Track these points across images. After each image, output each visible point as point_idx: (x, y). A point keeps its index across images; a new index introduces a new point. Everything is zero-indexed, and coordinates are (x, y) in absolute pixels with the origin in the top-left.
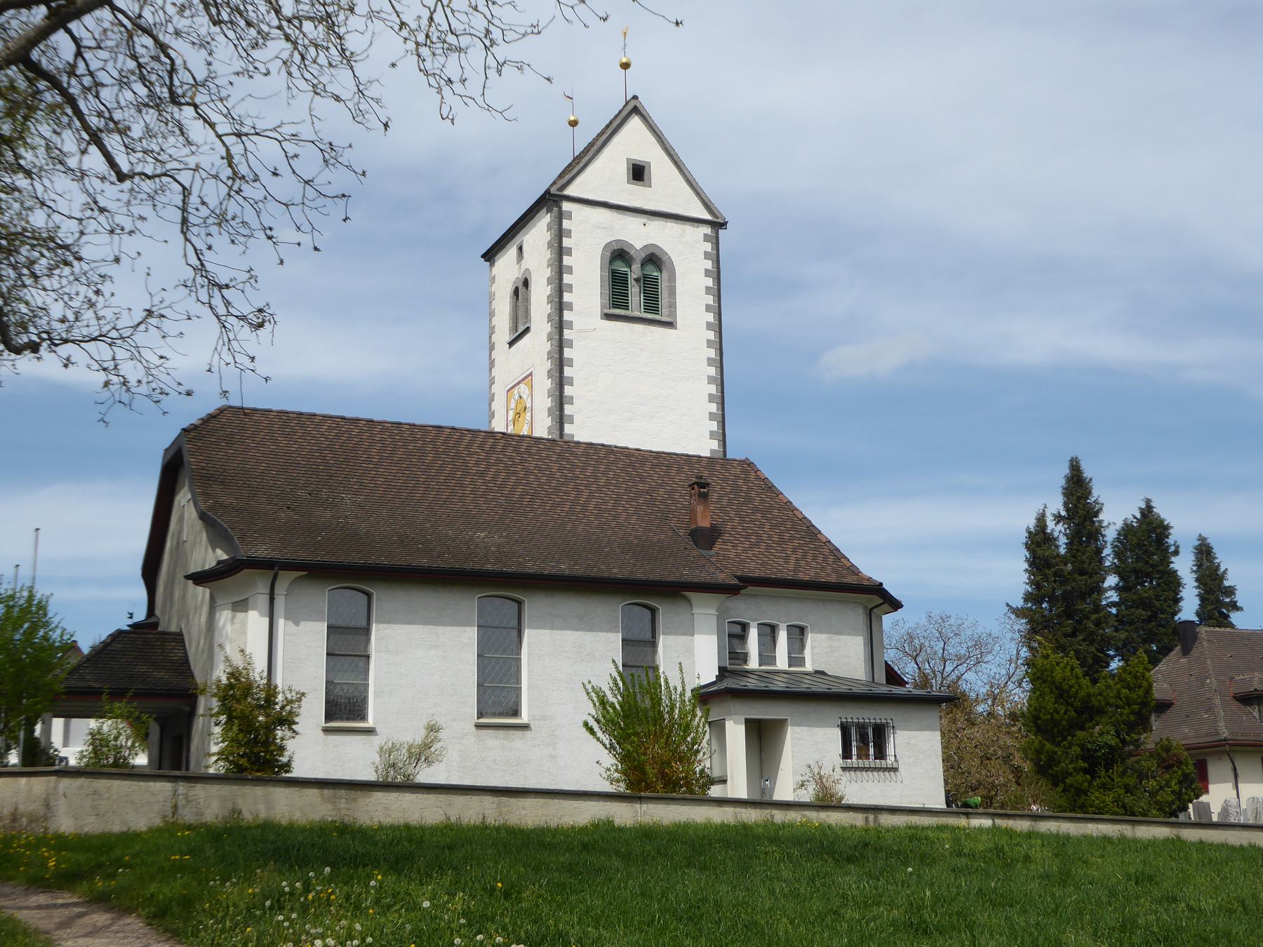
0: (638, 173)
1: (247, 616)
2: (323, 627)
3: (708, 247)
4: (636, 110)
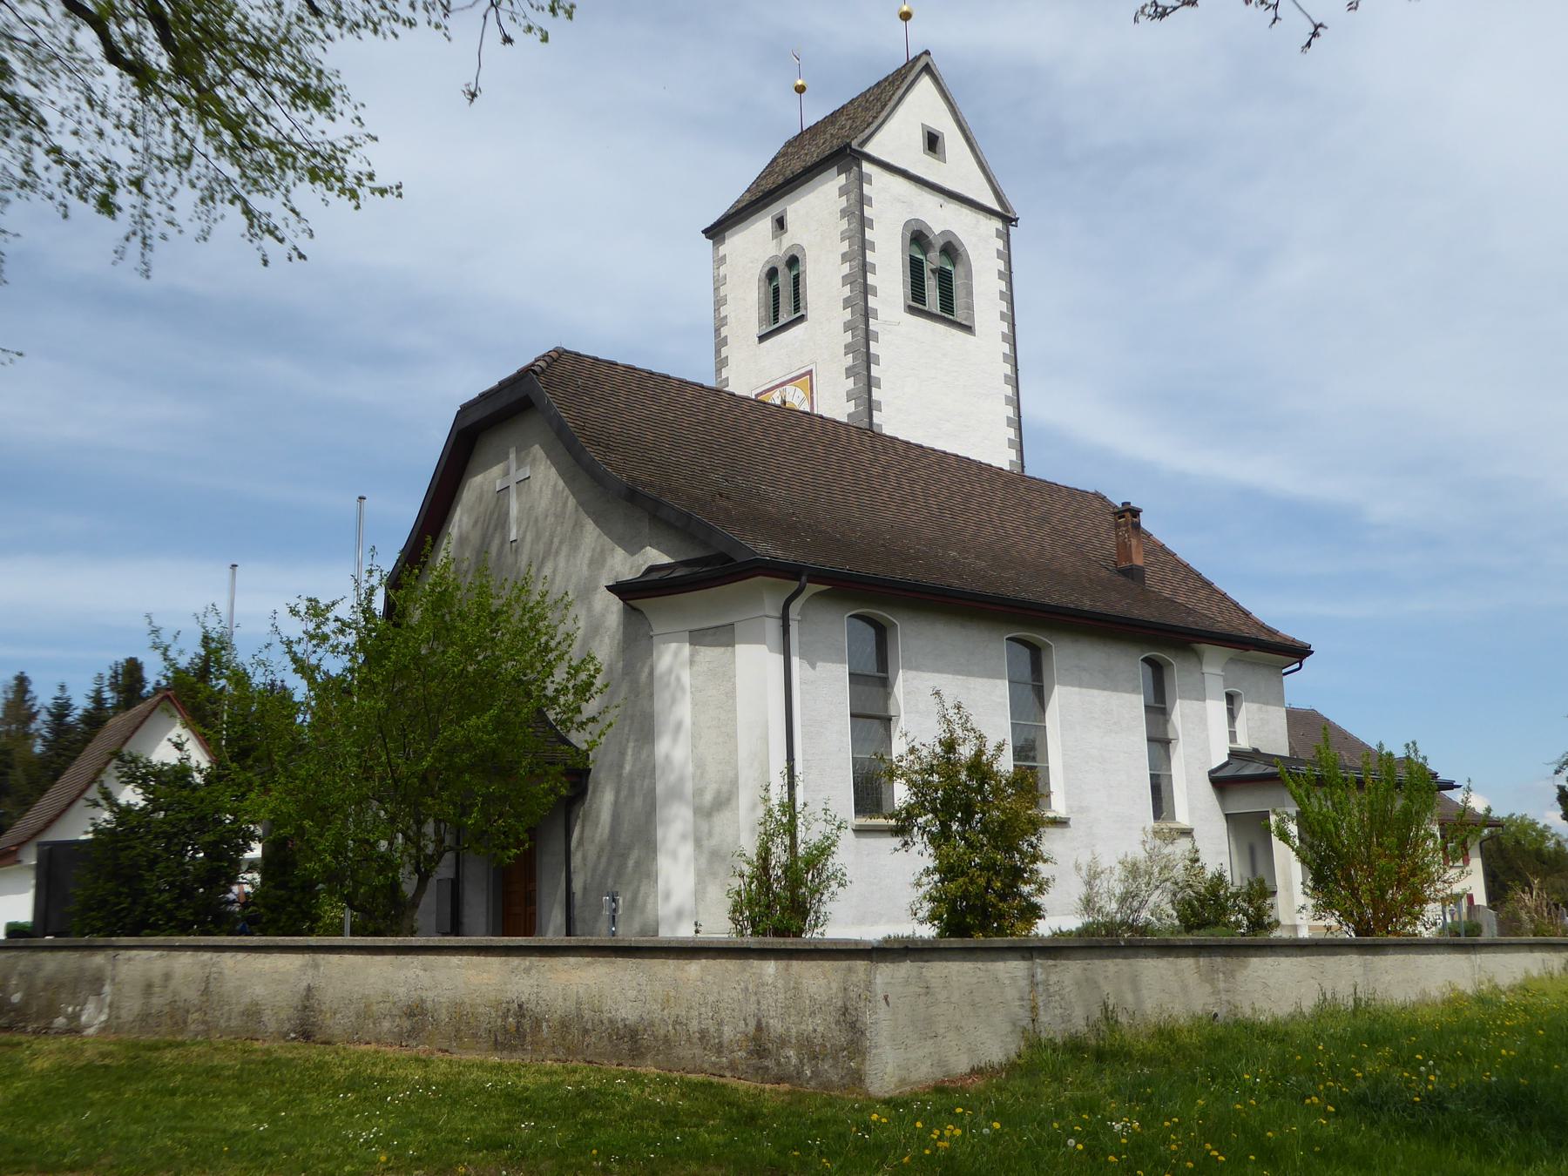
0: (933, 142)
1: (734, 652)
2: (843, 671)
3: (1000, 244)
4: (927, 69)
